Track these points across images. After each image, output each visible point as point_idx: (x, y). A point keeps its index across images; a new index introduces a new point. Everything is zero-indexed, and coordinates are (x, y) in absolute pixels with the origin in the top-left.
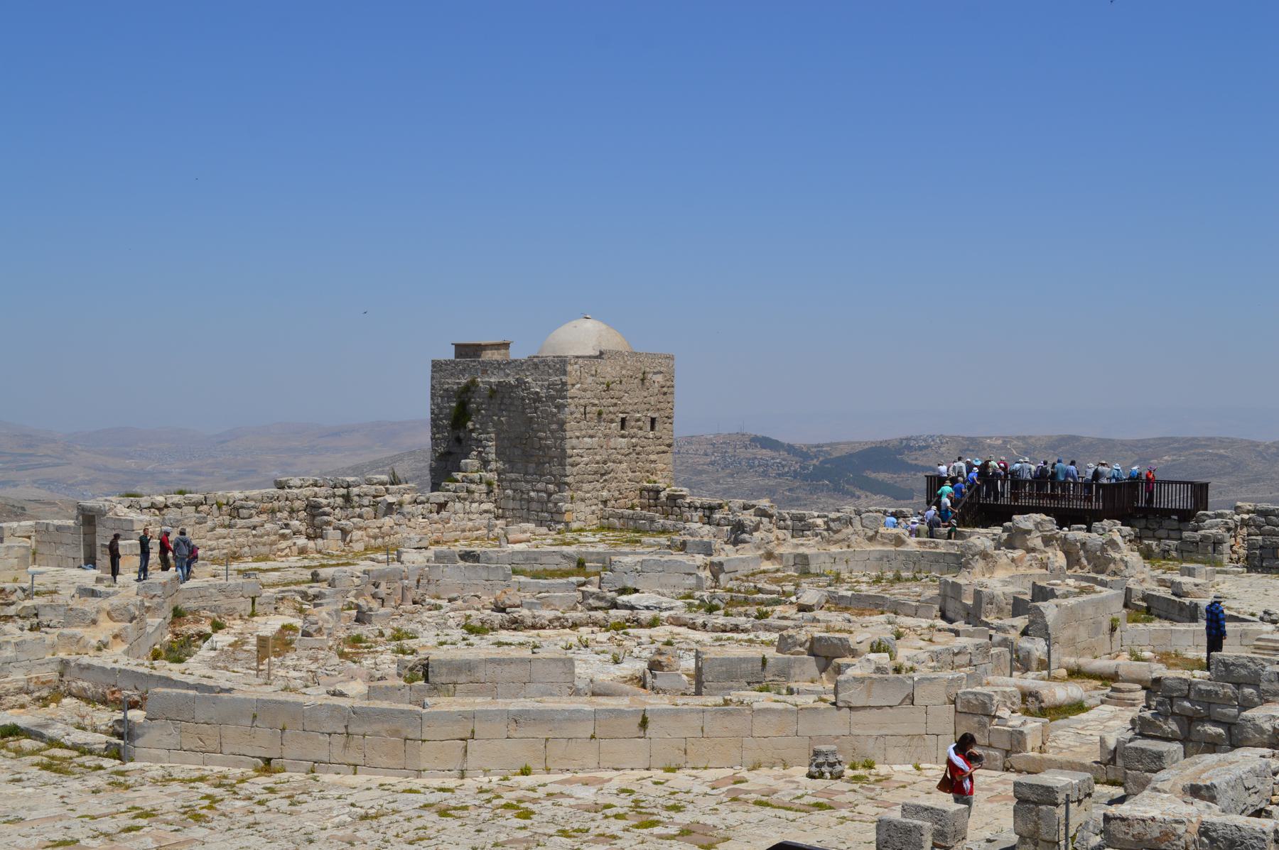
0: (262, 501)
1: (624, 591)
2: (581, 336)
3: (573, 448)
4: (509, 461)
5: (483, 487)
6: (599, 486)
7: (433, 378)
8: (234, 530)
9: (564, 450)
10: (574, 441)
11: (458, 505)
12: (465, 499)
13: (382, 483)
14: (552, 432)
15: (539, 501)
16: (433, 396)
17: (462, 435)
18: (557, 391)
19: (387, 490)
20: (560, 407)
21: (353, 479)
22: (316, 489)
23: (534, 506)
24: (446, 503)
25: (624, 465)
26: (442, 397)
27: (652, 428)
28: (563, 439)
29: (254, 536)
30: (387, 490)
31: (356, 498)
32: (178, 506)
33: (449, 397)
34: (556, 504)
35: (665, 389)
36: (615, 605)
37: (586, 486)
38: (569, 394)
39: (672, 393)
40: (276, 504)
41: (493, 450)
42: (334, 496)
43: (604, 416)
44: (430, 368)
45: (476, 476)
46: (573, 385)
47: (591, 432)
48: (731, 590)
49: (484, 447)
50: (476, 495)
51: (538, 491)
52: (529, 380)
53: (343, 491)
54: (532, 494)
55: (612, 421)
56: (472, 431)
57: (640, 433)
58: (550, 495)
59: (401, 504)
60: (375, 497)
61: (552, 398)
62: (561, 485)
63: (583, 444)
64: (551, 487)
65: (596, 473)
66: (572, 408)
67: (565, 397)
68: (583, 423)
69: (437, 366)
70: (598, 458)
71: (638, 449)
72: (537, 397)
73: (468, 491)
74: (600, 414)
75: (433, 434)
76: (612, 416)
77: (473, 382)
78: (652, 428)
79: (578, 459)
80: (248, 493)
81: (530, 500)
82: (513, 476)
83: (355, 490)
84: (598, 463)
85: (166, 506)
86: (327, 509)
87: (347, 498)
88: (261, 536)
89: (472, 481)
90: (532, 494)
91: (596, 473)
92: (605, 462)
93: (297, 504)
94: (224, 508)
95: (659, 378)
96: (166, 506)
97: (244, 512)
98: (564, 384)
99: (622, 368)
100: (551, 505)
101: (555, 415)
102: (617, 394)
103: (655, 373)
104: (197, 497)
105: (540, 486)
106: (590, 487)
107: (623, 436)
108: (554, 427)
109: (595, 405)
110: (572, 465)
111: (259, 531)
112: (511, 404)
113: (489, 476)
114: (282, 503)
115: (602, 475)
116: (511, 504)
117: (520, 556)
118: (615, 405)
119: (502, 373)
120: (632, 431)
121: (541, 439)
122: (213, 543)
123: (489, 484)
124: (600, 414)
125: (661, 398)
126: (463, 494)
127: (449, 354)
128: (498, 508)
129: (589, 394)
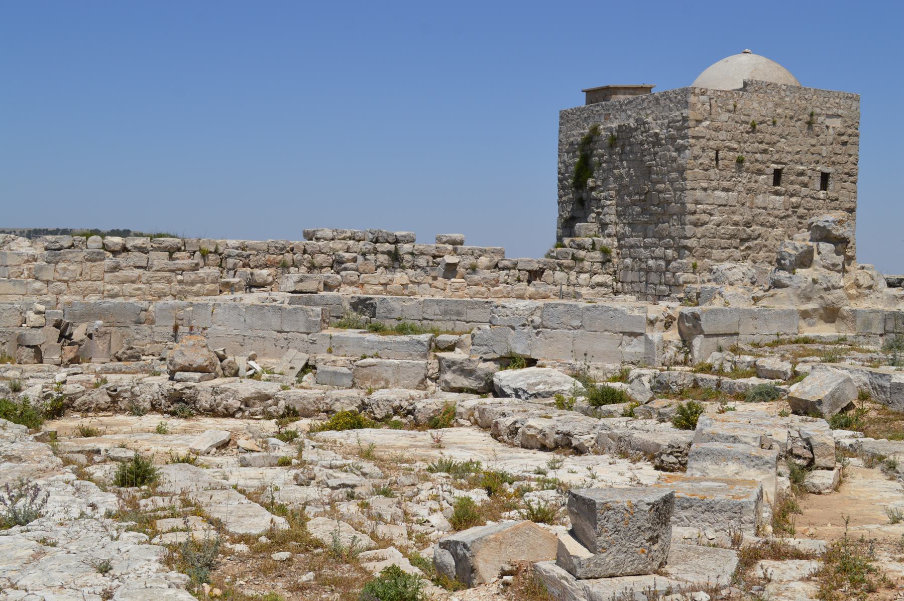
0: (268, 252)
1: (508, 361)
2: (730, 71)
3: (697, 203)
4: (629, 224)
5: (597, 255)
6: (737, 254)
7: (560, 131)
9: (683, 204)
10: (699, 194)
11: (559, 275)
12: (571, 268)
13: (454, 243)
14: (672, 182)
15: (660, 272)
16: (560, 151)
17: (584, 195)
18: (679, 129)
19: (455, 250)
20: (680, 149)
22: (351, 242)
23: (654, 277)
25: (779, 231)
26: (568, 153)
27: (824, 186)
28: (683, 190)
29: (180, 282)
30: (455, 250)
31: (408, 257)
32: (142, 250)
33: (574, 152)
34: (674, 273)
35: (845, 138)
36: (491, 389)
37: (716, 253)
38: (690, 132)
39: (856, 144)
40: (289, 257)
41: (613, 210)
42: (376, 252)
43: (747, 165)
44: (558, 120)
45: (588, 241)
46: (699, 122)
47: (725, 184)
48: (708, 369)
49: (603, 207)
50: (587, 264)
51: (656, 258)
52: (650, 119)
53: (387, 247)
54: (651, 262)
55: (760, 172)
56: (593, 189)
57: (804, 191)
58: (668, 262)
60: (434, 257)
61: (672, 139)
62: (681, 250)
63: (711, 198)
64: (669, 252)
65: (732, 237)
66: (697, 151)
67: (685, 137)
68: (712, 172)
69: (565, 117)
70: (736, 218)
71: (801, 211)
72: (657, 141)
73: (574, 258)
74: (740, 161)
75: (560, 197)
76: (760, 166)
77: (595, 130)
78: (824, 186)
79: (705, 217)
80: (248, 242)
81: (648, 270)
82: (632, 241)
83: (407, 247)
84: (736, 224)
85: (125, 249)
86: (348, 265)
87: (395, 257)
88: (193, 283)
89: (581, 247)
90: (651, 262)
91: (732, 237)
92: (748, 224)
93: (319, 259)
94: (212, 257)
95: (837, 123)
96: (125, 249)
97: (231, 262)
98: (685, 119)
99: (777, 105)
100: (669, 275)
101: (674, 160)
102: (768, 138)
103: (828, 116)
104: (168, 241)
105: (659, 252)
106: (725, 254)
107: (777, 193)
108: (674, 175)
109: (734, 149)
110: (696, 224)
111: (189, 276)
112: (631, 152)
113: (606, 241)
114: (298, 257)
115: (743, 241)
116: (630, 277)
118: (765, 151)
119: (623, 114)
120: (791, 188)
121: (660, 192)
122: (117, 288)
123: (605, 252)
124: (740, 161)
125: (838, 148)
126: (567, 262)
127: (581, 101)
128: (617, 281)
129: (723, 135)
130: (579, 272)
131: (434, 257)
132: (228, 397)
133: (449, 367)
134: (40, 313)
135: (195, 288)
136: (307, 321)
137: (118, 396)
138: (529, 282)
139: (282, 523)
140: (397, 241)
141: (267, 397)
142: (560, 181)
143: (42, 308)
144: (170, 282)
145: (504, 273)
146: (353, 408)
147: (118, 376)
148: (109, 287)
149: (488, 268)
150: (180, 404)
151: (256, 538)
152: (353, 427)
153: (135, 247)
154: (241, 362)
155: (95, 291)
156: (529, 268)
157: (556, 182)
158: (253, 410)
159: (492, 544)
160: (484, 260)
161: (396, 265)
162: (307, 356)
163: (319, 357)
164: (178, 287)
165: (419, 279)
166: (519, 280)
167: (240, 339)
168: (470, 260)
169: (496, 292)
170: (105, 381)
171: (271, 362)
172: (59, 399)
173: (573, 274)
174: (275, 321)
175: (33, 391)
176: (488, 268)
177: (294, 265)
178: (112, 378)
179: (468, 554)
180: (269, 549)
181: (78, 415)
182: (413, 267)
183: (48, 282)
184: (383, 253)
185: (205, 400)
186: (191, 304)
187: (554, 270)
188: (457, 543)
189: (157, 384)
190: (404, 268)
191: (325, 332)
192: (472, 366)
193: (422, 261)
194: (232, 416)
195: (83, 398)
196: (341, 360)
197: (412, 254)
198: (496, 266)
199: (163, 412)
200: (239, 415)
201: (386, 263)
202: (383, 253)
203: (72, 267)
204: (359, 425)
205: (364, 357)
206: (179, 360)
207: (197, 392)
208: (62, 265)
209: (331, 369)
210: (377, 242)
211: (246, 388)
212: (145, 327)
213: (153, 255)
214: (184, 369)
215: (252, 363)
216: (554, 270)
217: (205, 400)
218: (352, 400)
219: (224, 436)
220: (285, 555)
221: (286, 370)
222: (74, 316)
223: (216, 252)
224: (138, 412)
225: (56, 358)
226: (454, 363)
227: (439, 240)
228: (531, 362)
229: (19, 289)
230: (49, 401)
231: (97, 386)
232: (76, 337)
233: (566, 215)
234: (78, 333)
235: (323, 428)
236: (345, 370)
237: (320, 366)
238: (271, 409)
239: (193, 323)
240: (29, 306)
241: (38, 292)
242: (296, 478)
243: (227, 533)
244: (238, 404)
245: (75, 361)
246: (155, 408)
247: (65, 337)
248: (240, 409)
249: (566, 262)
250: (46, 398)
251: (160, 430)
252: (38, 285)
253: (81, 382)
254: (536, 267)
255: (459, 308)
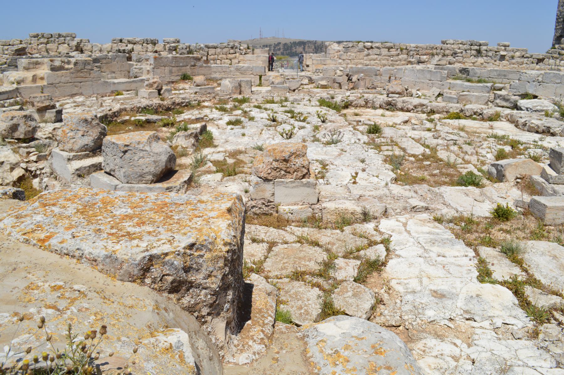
1: (525, 96)
8: (380, 57)
11: (551, 61)
12: (557, 58)
13: (505, 46)
19: (505, 49)
21: (483, 42)
22: (461, 45)
24: (543, 59)
29: (392, 60)
31: (485, 52)
32: (378, 48)
36: (516, 107)
40: (435, 51)
42: (471, 49)
59: (513, 57)
60: (496, 52)
73: (559, 54)
75: (556, 26)
80: (419, 45)
83: (484, 48)
85: (372, 48)
86: (459, 55)
87: (479, 52)
88: (396, 61)
93: (447, 52)
94: (404, 51)
96: (372, 48)
97: (412, 53)
104: (388, 45)
114: (438, 51)
117: (495, 73)
122: (368, 62)
130: (561, 60)
131: (496, 52)
132: (408, 104)
133: (499, 97)
134: (341, 71)
135: (397, 63)
136: (441, 76)
137: (368, 102)
138: (537, 64)
139: (427, 151)
140: (480, 45)
141: (423, 105)
142: (557, 19)
143: (342, 69)
144: (388, 60)
145: (526, 59)
146: (458, 111)
147: (368, 95)
148: (365, 62)
149: (519, 57)
150: (390, 106)
151: (418, 156)
152: (456, 118)
153: (376, 47)
154: (414, 91)
155: (361, 63)
156: (538, 58)
157: (555, 20)
158: (417, 110)
159: (513, 166)
160: (518, 54)
161: (479, 55)
162: (440, 90)
163: (445, 91)
164: (391, 62)
165: (488, 61)
166: (533, 63)
167: (414, 83)
168: (512, 54)
169: (521, 68)
170: (363, 96)
171: (425, 92)
172: (347, 102)
173: (558, 60)
174: (428, 76)
175: (338, 99)
176: (519, 57)
177: (437, 54)
178: (366, 96)
179: (502, 169)
180: (422, 160)
181: (353, 108)
182: (486, 56)
183: (344, 60)
184: (474, 50)
185: (400, 105)
186: (396, 69)
187: (549, 59)
188: (498, 165)
189: (383, 98)
190: (482, 56)
191: (448, 81)
192: (509, 97)
193: (490, 54)
194: (410, 111)
195: (356, 102)
196: (454, 92)
197: (486, 50)
198: (523, 56)
199: (384, 109)
200: (412, 111)
201: (475, 54)
202: (474, 50)
203: (353, 54)
204: (459, 118)
205: (463, 92)
206: (391, 90)
207: (397, 102)
208: (349, 54)
209: (448, 95)
210: (472, 45)
211: (416, 101)
212: (378, 77)
213: (382, 50)
214: (392, 93)
215: (418, 92)
216: (549, 59)
217: (400, 105)
218: (457, 108)
219: (406, 119)
220: (428, 163)
221: (431, 95)
222: (353, 72)
223: (406, 49)
224: (374, 108)
225: (346, 87)
226: (501, 96)
227: (499, 45)
228: (535, 97)
229: (334, 62)
230: (344, 103)
231: (360, 98)
232: (353, 80)
233: (558, 35)
234: (354, 79)
235: (445, 118)
236: (455, 96)
237: (445, 94)
238: (425, 110)
239: (397, 76)
240: (338, 68)
241: (340, 64)
242: (433, 136)
243: (407, 153)
244: (412, 107)
245: (353, 89)
246: (381, 107)
247: (349, 80)
248: (413, 109)
249: (555, 55)
250: (342, 101)
251: (383, 115)
252: (340, 61)
253: (355, 96)
254: (541, 57)
255: (505, 73)
